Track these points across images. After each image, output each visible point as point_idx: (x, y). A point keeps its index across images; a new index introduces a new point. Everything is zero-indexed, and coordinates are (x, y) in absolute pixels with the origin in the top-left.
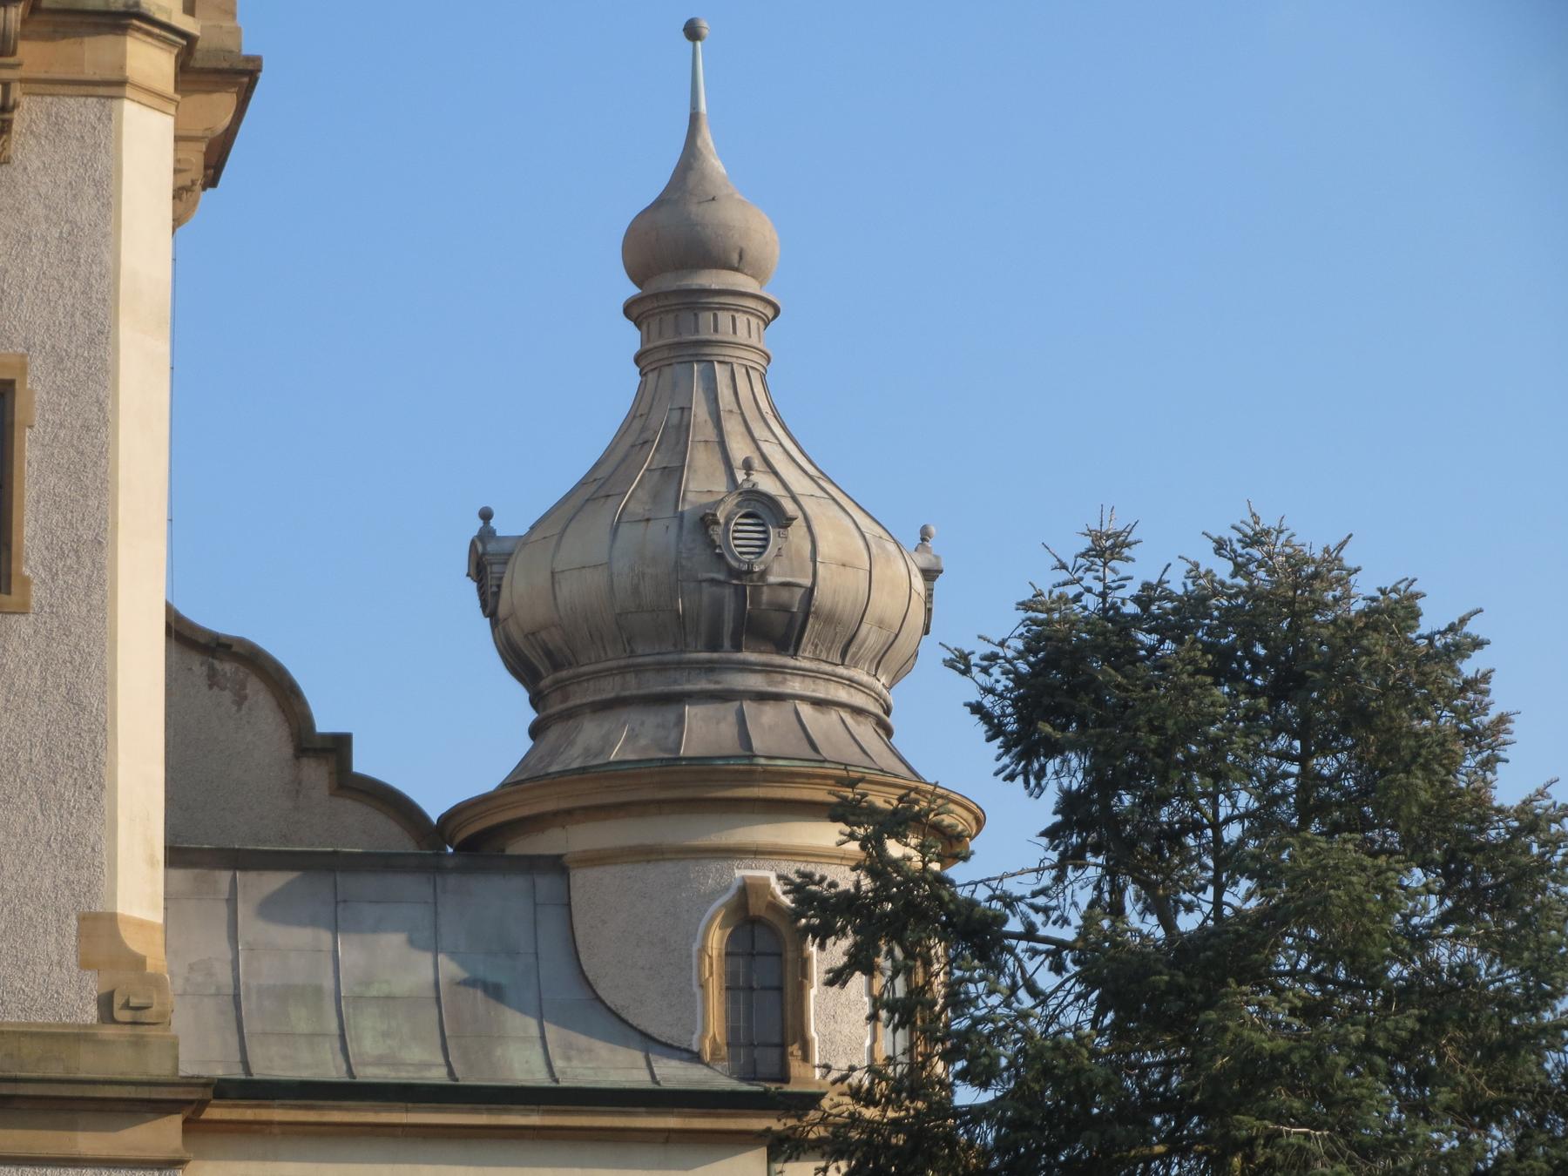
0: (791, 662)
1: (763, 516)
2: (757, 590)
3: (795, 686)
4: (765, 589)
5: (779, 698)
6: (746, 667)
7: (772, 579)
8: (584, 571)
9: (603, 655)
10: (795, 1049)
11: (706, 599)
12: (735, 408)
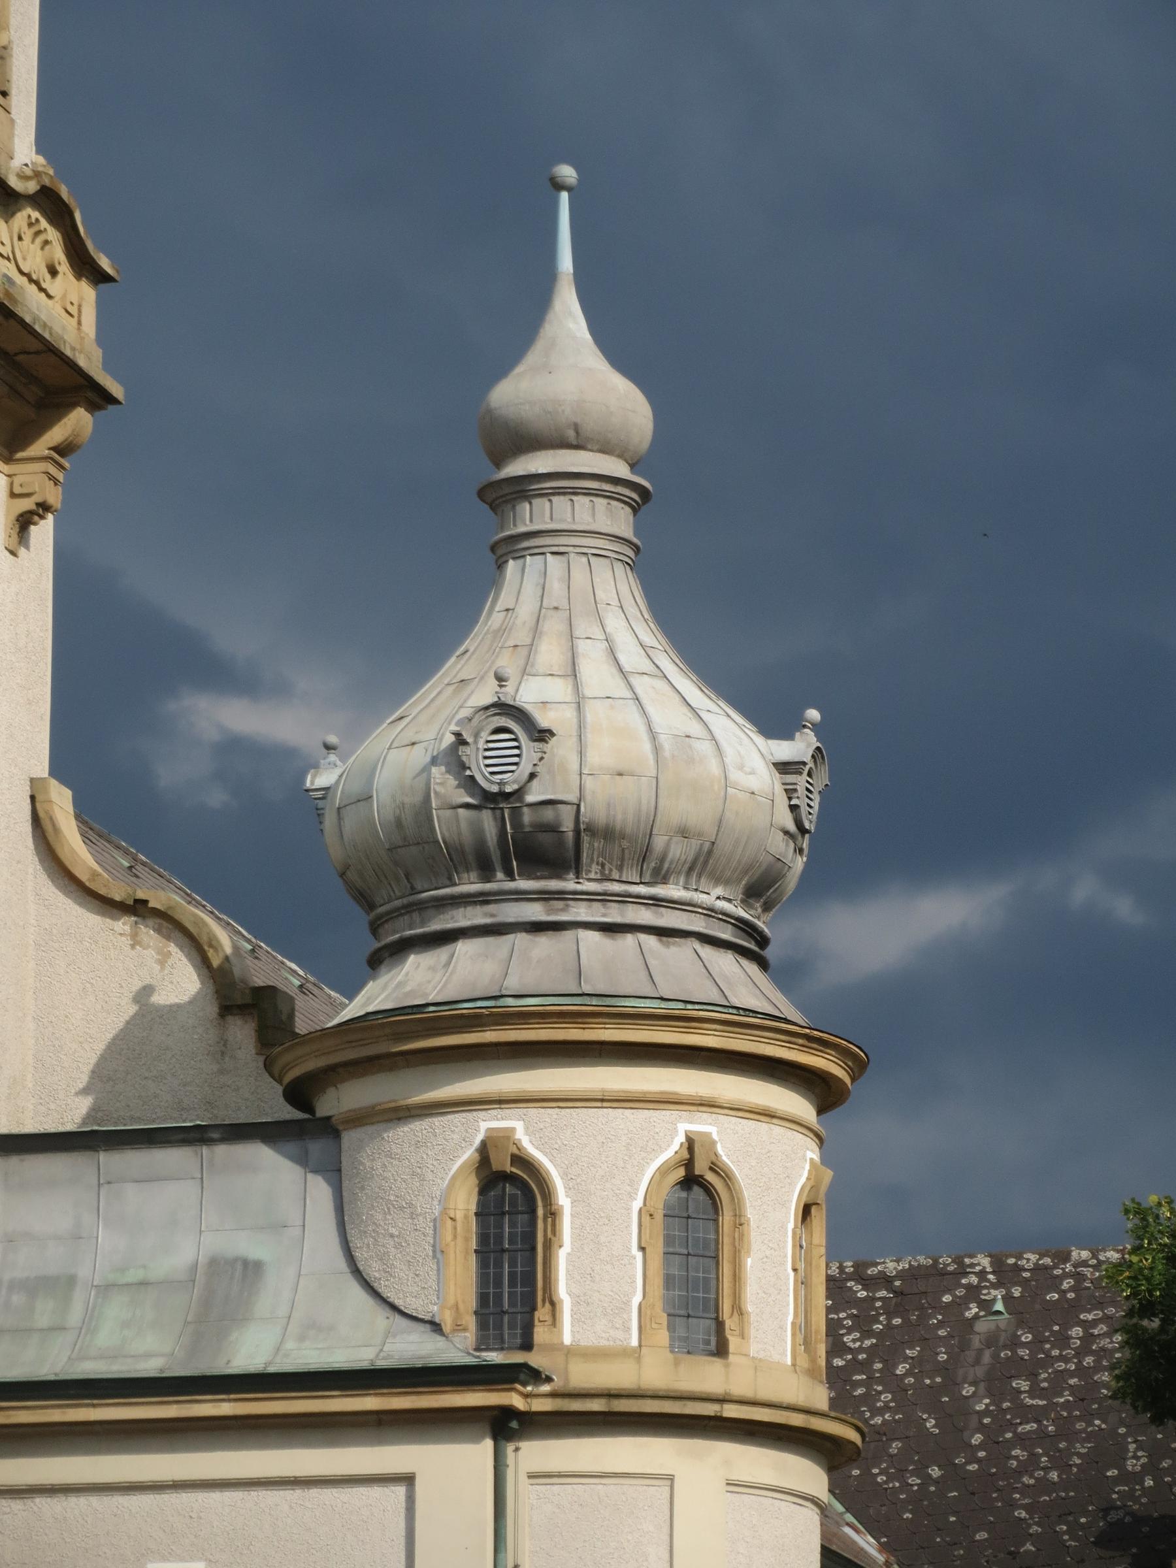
0: (570, 885)
1: (515, 730)
2: (516, 813)
3: (581, 912)
4: (525, 810)
5: (557, 927)
6: (521, 896)
7: (530, 798)
8: (358, 803)
9: (392, 894)
10: (542, 1313)
11: (464, 826)
12: (564, 604)
